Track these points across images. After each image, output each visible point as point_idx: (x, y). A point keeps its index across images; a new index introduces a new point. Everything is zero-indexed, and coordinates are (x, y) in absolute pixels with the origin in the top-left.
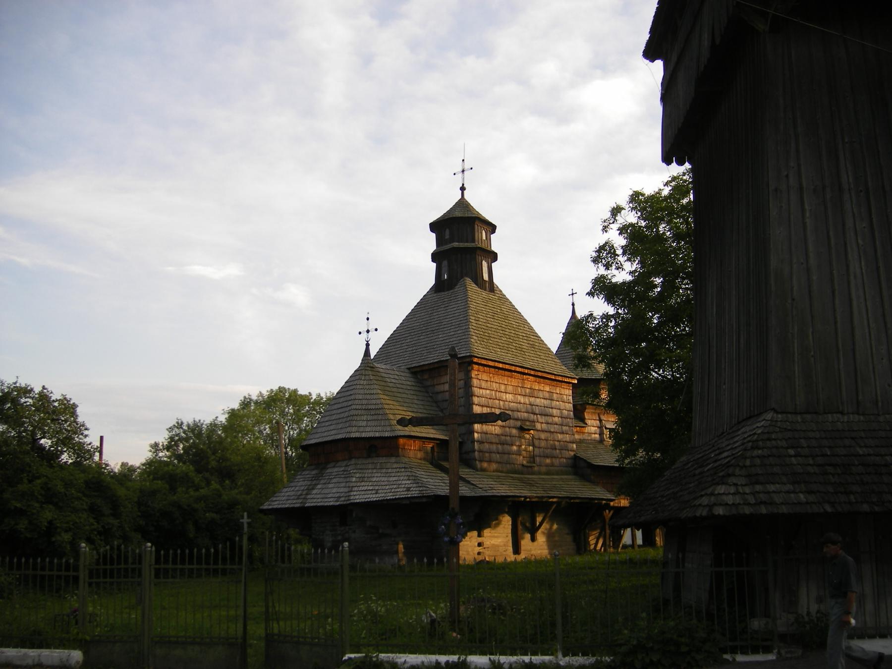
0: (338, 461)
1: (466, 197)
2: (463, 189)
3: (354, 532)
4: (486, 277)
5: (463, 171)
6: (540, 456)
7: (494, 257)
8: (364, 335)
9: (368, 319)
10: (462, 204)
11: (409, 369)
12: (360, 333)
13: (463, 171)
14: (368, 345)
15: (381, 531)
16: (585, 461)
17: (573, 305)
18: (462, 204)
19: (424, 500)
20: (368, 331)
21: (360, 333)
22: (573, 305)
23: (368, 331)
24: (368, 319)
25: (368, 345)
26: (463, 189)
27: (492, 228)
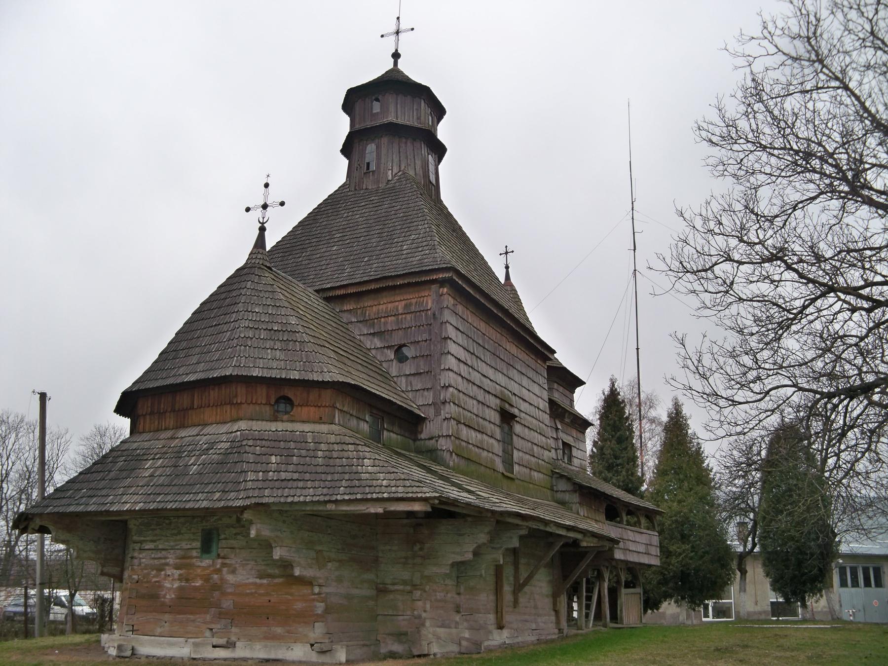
0: (205, 425)
1: (400, 67)
2: (396, 56)
3: (233, 572)
4: (432, 178)
5: (397, 33)
6: (519, 464)
7: (439, 150)
8: (257, 214)
9: (267, 185)
10: (395, 70)
11: (317, 291)
12: (248, 210)
13: (397, 33)
14: (262, 229)
15: (297, 572)
16: (569, 479)
17: (507, 267)
18: (395, 70)
19: (417, 507)
20: (265, 207)
21: (248, 210)
22: (507, 267)
23: (265, 207)
24: (267, 185)
25: (262, 229)
26: (396, 56)
27: (439, 111)
